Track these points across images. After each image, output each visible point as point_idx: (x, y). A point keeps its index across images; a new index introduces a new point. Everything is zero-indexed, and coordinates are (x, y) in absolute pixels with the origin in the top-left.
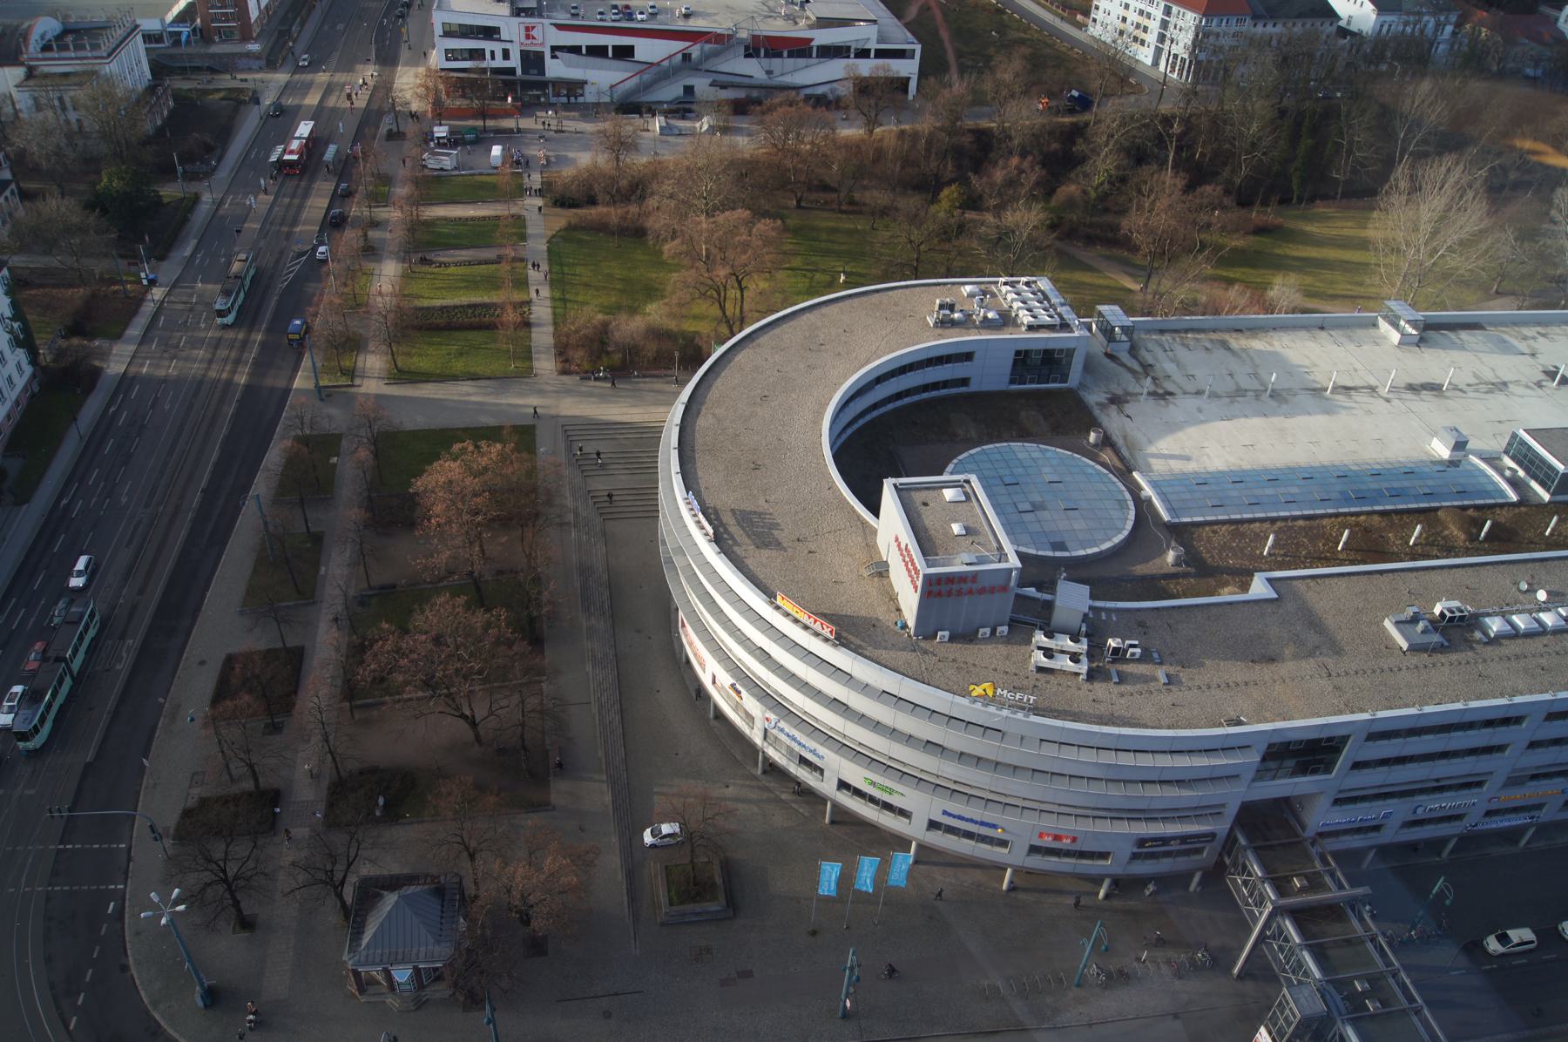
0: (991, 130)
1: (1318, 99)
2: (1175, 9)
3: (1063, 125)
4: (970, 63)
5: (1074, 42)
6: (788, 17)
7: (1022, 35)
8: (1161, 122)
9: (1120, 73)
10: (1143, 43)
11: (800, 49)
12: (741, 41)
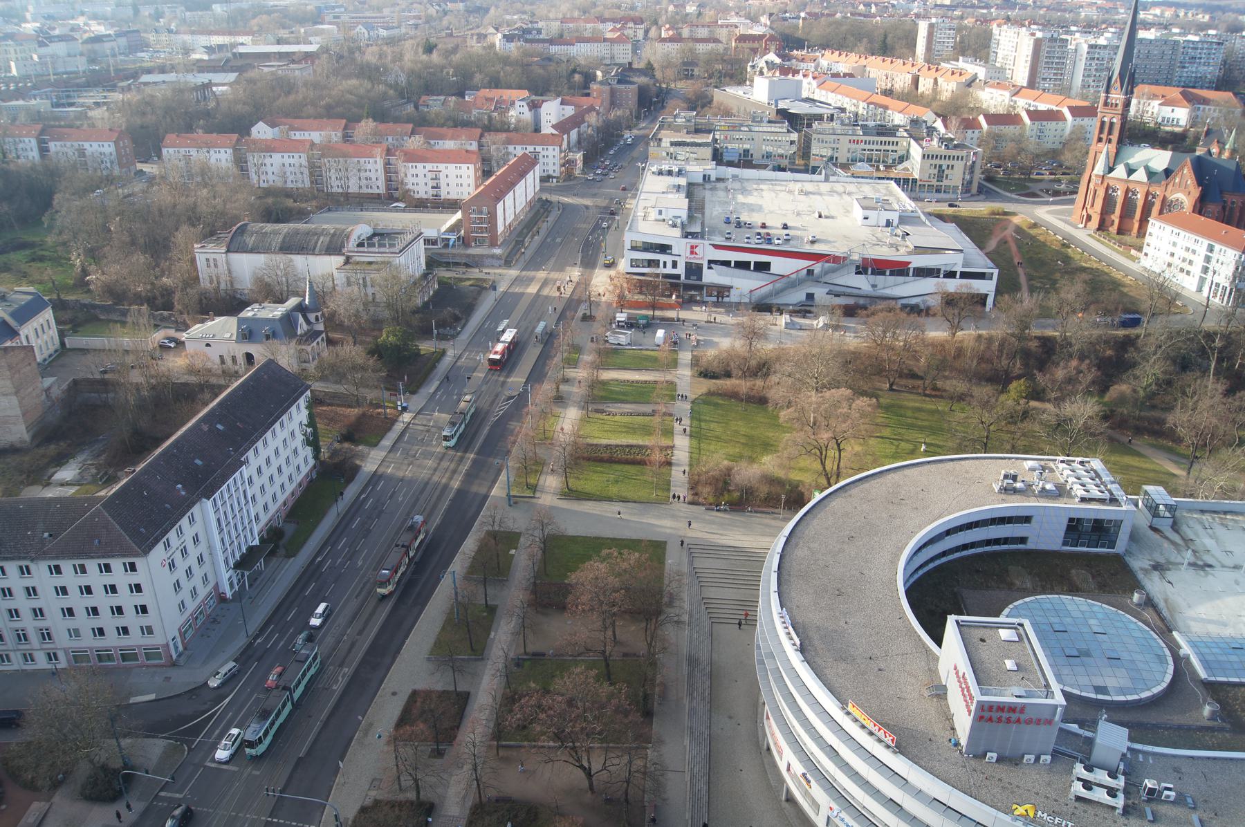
0: (1055, 338)
3: (1116, 337)
4: (1039, 285)
5: (1128, 272)
6: (891, 245)
8: (1204, 337)
9: (1166, 298)
10: (1188, 273)
11: (899, 269)
12: (852, 262)
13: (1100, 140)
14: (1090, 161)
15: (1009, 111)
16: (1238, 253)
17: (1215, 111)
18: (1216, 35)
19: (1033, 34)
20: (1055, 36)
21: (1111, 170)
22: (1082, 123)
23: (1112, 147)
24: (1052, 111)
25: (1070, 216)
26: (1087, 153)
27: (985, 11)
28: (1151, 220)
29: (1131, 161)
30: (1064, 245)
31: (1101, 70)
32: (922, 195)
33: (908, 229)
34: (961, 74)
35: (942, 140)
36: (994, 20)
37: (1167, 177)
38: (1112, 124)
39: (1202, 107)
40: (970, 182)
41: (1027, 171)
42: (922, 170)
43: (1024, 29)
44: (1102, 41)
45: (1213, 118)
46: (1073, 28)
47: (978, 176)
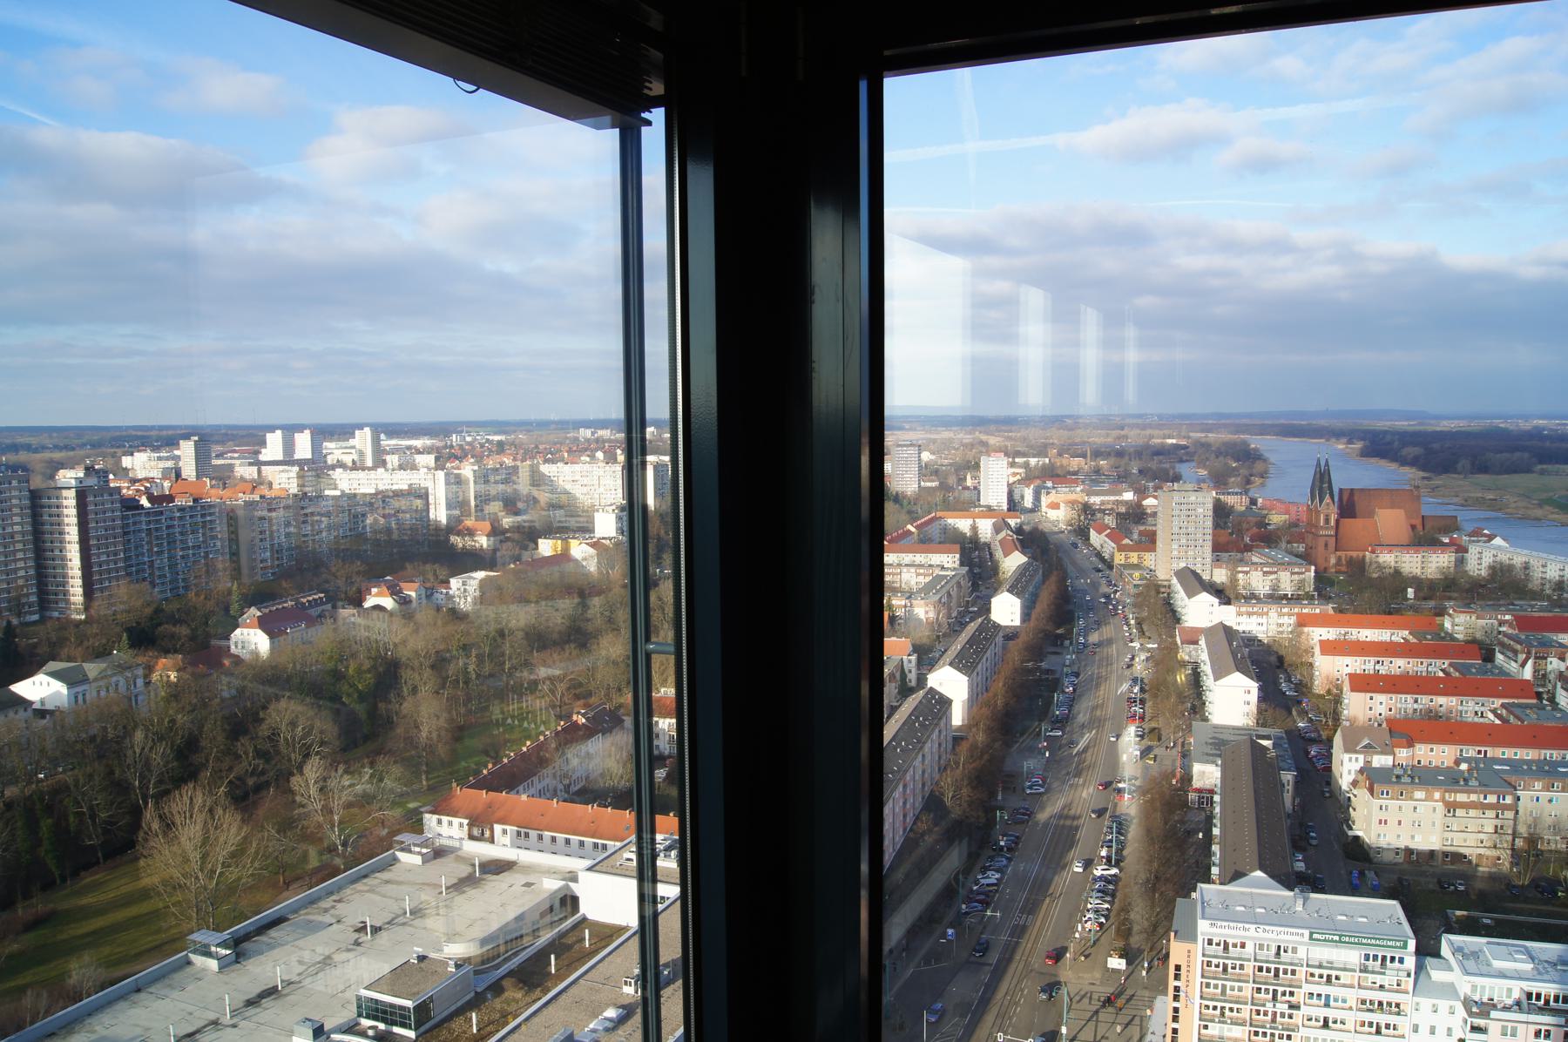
1: (42, 780)
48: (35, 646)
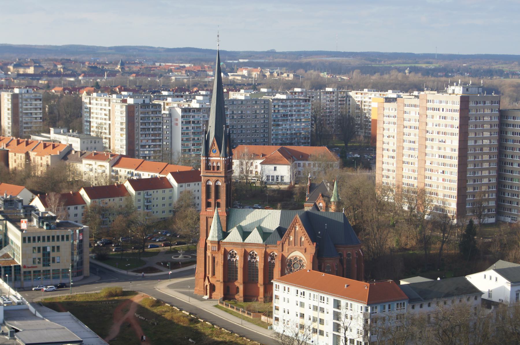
2: (343, 302)
7: (216, 339)
10: (321, 333)
13: (208, 205)
14: (203, 228)
15: (111, 182)
16: (364, 305)
17: (314, 165)
18: (302, 92)
19: (124, 101)
20: (147, 101)
21: (225, 234)
22: (188, 188)
23: (222, 210)
24: (156, 178)
25: (193, 288)
26: (199, 219)
27: (72, 79)
28: (275, 283)
29: (243, 224)
30: (192, 320)
31: (199, 133)
32: (26, 284)
33: (16, 324)
34: (54, 147)
35: (42, 219)
36: (83, 87)
37: (281, 235)
38: (217, 187)
39: (302, 163)
40: (81, 263)
41: (141, 244)
42: (24, 255)
43: (114, 96)
44: (194, 104)
45: (314, 173)
46: (165, 93)
47: (88, 254)
48: (489, 244)
